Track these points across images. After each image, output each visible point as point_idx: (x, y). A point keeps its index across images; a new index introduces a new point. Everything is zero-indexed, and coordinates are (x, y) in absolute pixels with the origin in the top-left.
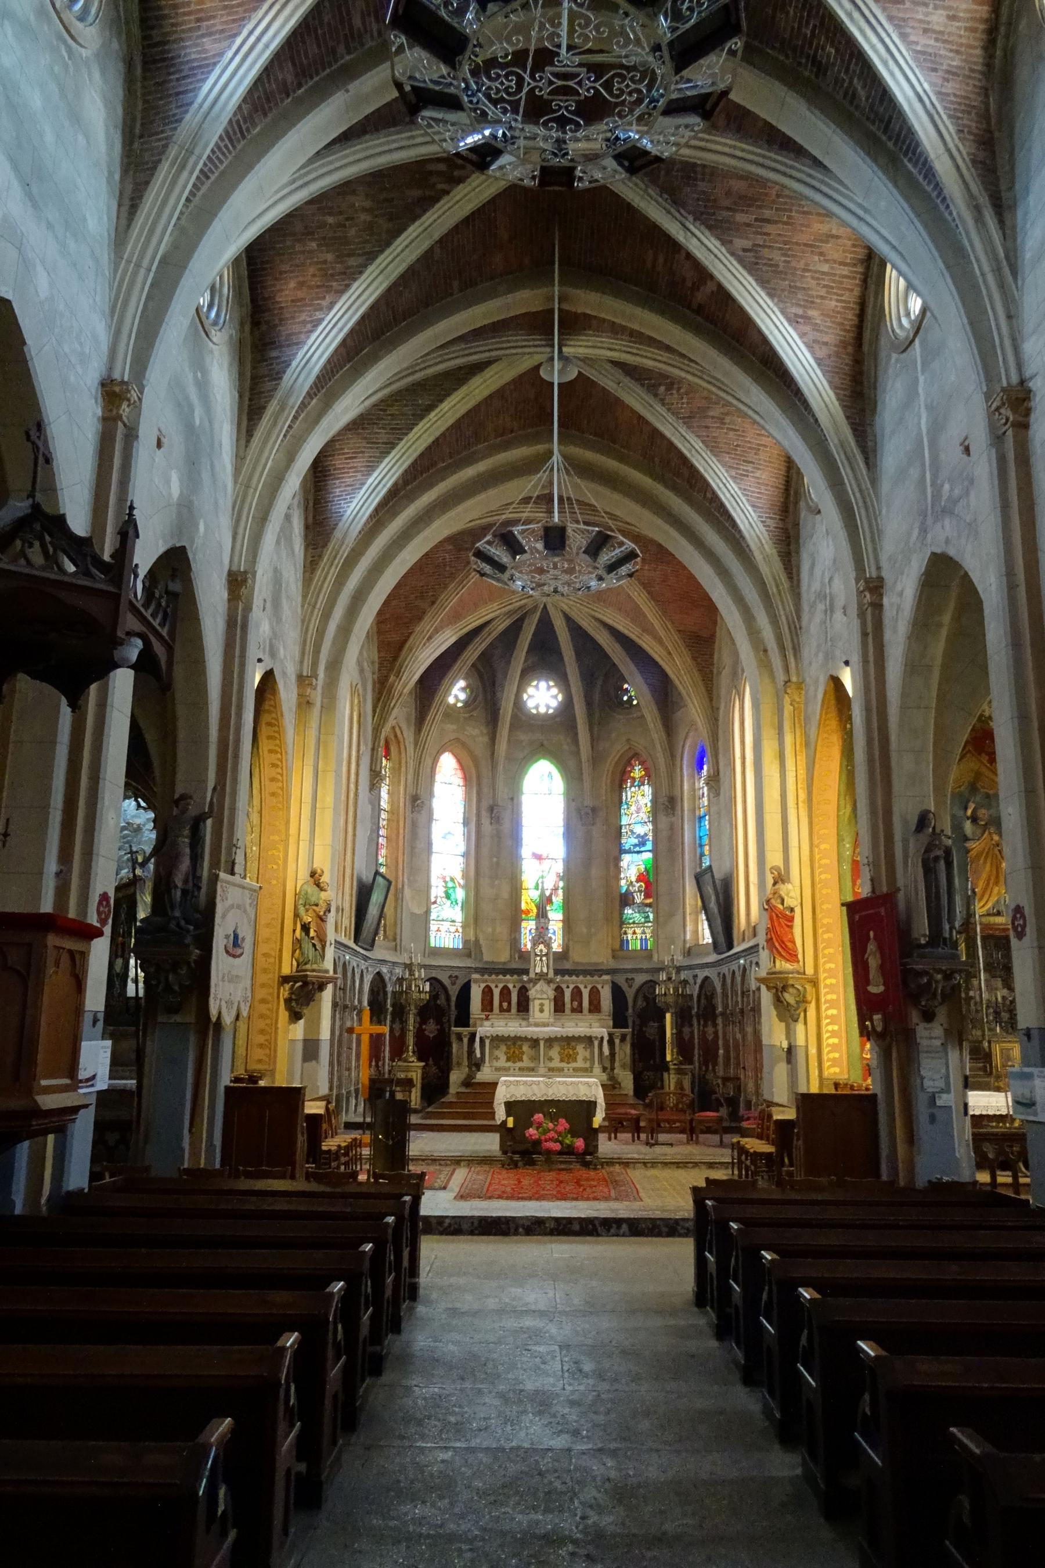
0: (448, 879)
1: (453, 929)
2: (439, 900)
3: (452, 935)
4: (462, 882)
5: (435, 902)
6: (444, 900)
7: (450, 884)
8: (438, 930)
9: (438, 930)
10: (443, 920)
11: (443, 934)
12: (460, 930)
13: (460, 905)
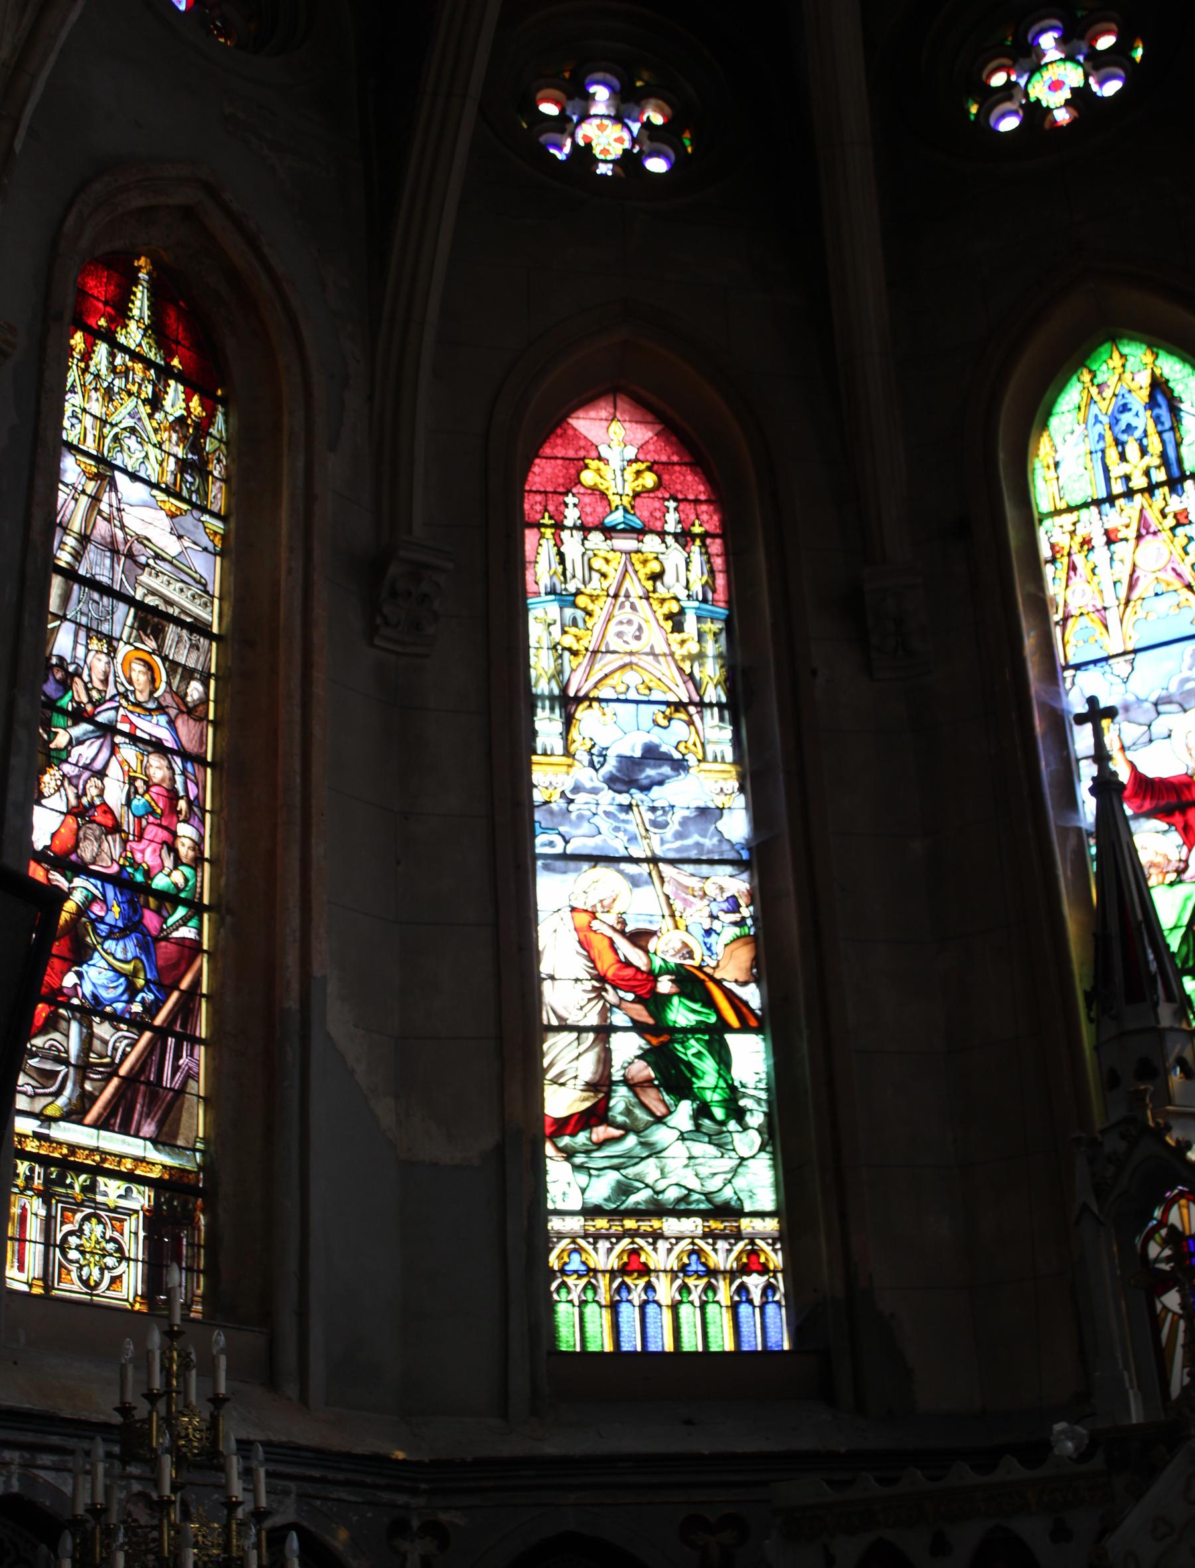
0: (665, 985)
1: (722, 1257)
2: (620, 1099)
3: (725, 1292)
4: (752, 995)
5: (596, 1115)
6: (651, 1098)
7: (681, 1014)
8: (631, 1266)
9: (631, 1266)
10: (658, 1209)
11: (665, 1290)
12: (776, 1260)
13: (756, 1119)
